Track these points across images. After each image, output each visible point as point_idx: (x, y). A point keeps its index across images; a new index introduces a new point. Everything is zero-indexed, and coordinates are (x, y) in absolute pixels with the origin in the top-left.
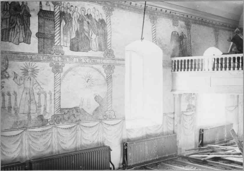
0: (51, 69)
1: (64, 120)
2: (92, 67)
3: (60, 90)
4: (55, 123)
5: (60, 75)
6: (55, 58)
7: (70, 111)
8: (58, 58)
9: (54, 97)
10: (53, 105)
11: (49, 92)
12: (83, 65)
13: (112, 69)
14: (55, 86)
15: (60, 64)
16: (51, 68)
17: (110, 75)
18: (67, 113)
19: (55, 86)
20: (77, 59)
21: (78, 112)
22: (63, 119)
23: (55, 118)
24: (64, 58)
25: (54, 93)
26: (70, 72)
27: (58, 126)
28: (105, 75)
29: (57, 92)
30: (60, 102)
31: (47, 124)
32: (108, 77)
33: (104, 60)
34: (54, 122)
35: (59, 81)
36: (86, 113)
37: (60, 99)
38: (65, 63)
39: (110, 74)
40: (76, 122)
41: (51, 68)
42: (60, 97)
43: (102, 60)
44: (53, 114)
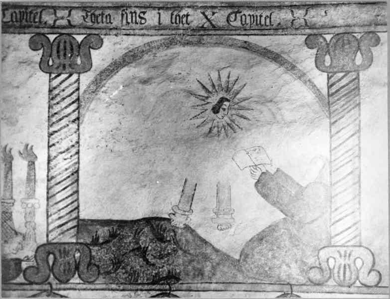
0: (38, 59)
1: (95, 268)
2: (247, 47)
3: (78, 143)
4: (52, 276)
5: (78, 80)
6: (55, 14)
7: (126, 231)
8: (70, 15)
9: (49, 171)
10: (44, 202)
11: (22, 149)
12: (195, 39)
13: (359, 48)
14: (50, 126)
15: (79, 38)
16: (37, 56)
17: (353, 75)
18: (106, 242)
19: (50, 126)
20: (166, 18)
21: (162, 239)
22: (89, 264)
23: (51, 256)
24: (98, 12)
25: (49, 157)
26: (126, 68)
27: (62, 293)
28: (321, 80)
29: (61, 153)
30: (77, 192)
31: (14, 278)
32: (333, 90)
33: (312, 12)
34: (44, 271)
35: (74, 106)
36: (209, 251)
37: (77, 181)
38: (104, 32)
39: (348, 73)
40: (153, 283)
41: (37, 56)
42: (77, 172)
43: (299, 13)
44: (44, 241)
